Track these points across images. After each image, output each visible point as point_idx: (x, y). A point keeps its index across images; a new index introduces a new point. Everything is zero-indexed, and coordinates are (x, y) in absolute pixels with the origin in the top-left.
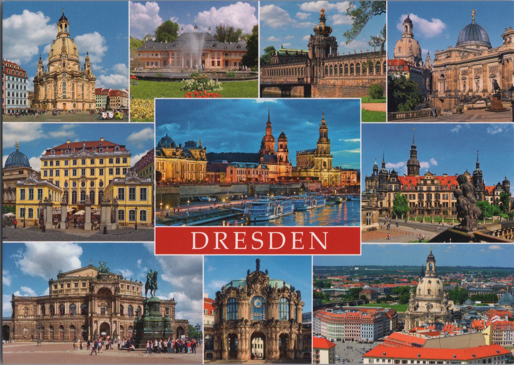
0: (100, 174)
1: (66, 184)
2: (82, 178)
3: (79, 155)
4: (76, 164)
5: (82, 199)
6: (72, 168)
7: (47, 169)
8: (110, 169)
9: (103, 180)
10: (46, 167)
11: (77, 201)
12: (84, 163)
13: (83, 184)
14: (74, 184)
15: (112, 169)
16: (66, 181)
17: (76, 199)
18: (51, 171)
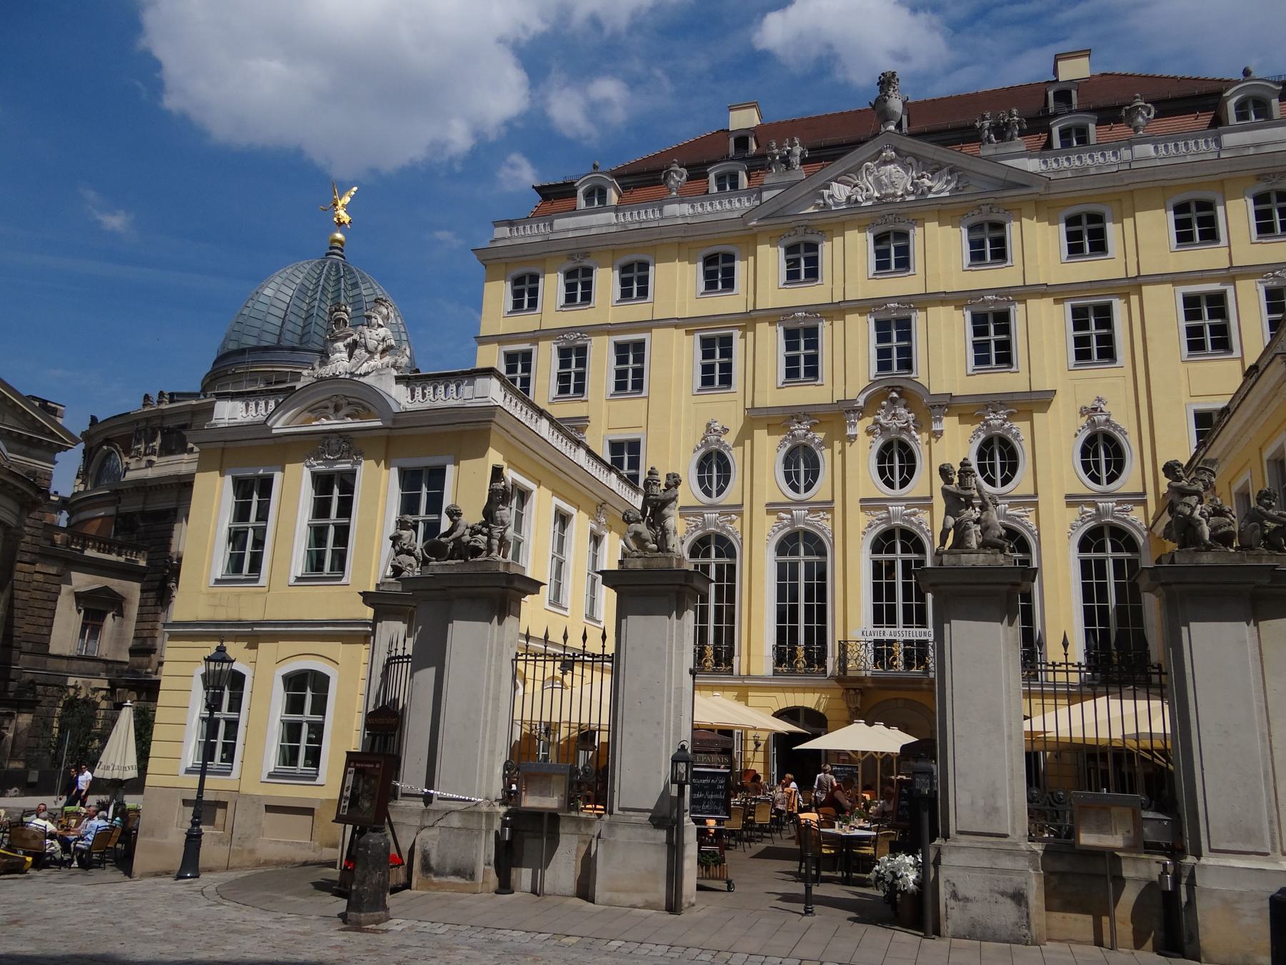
0: (1082, 354)
1: (714, 466)
2: (879, 398)
3: (840, 191)
4: (813, 274)
5: (882, 615)
6: (773, 316)
7: (537, 336)
8: (1192, 305)
9: (1121, 417)
10: (526, 322)
11: (834, 635)
12: (893, 252)
14: (802, 466)
15: (1217, 303)
17: (818, 613)
18: (573, 356)
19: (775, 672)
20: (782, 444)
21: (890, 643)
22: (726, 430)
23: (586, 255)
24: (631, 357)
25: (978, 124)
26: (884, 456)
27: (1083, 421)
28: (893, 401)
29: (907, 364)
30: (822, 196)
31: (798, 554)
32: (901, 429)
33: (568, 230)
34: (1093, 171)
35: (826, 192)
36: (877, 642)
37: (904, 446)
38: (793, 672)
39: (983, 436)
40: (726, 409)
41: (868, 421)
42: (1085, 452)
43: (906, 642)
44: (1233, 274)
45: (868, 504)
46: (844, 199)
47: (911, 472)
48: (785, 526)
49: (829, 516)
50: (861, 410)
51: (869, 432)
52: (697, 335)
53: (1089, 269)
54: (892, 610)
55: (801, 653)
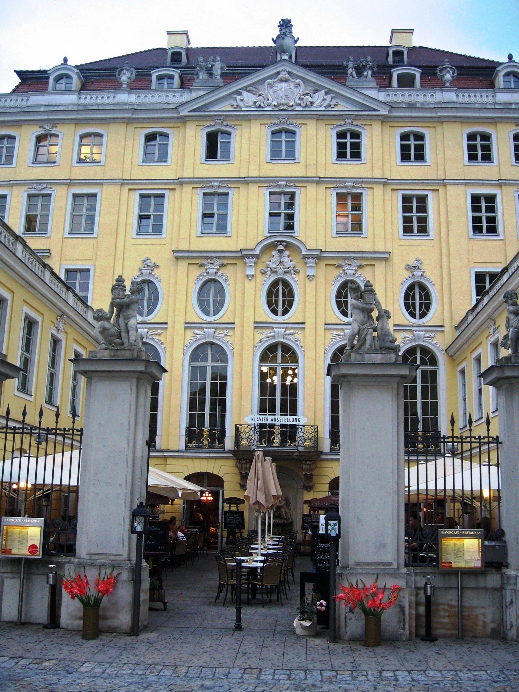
0: (407, 230)
3: (248, 98)
5: (266, 407)
13: (280, 296)
16: (149, 266)
17: (220, 404)
19: (187, 446)
20: (198, 279)
21: (272, 426)
22: (157, 266)
23: (54, 126)
24: (85, 205)
25: (345, 63)
26: (271, 293)
27: (407, 274)
28: (281, 251)
29: (290, 227)
30: (236, 99)
31: (206, 361)
32: (285, 272)
33: (41, 106)
34: (418, 106)
35: (238, 97)
36: (262, 426)
37: (286, 284)
38: (199, 448)
39: (342, 280)
40: (157, 249)
41: (261, 266)
42: (407, 296)
43: (282, 426)
44: (500, 183)
45: (259, 325)
46: (251, 104)
47: (291, 304)
48: (199, 339)
49: (231, 332)
50: (257, 257)
51: (264, 273)
52: (138, 193)
53: (412, 171)
54: (273, 403)
55: (206, 433)
